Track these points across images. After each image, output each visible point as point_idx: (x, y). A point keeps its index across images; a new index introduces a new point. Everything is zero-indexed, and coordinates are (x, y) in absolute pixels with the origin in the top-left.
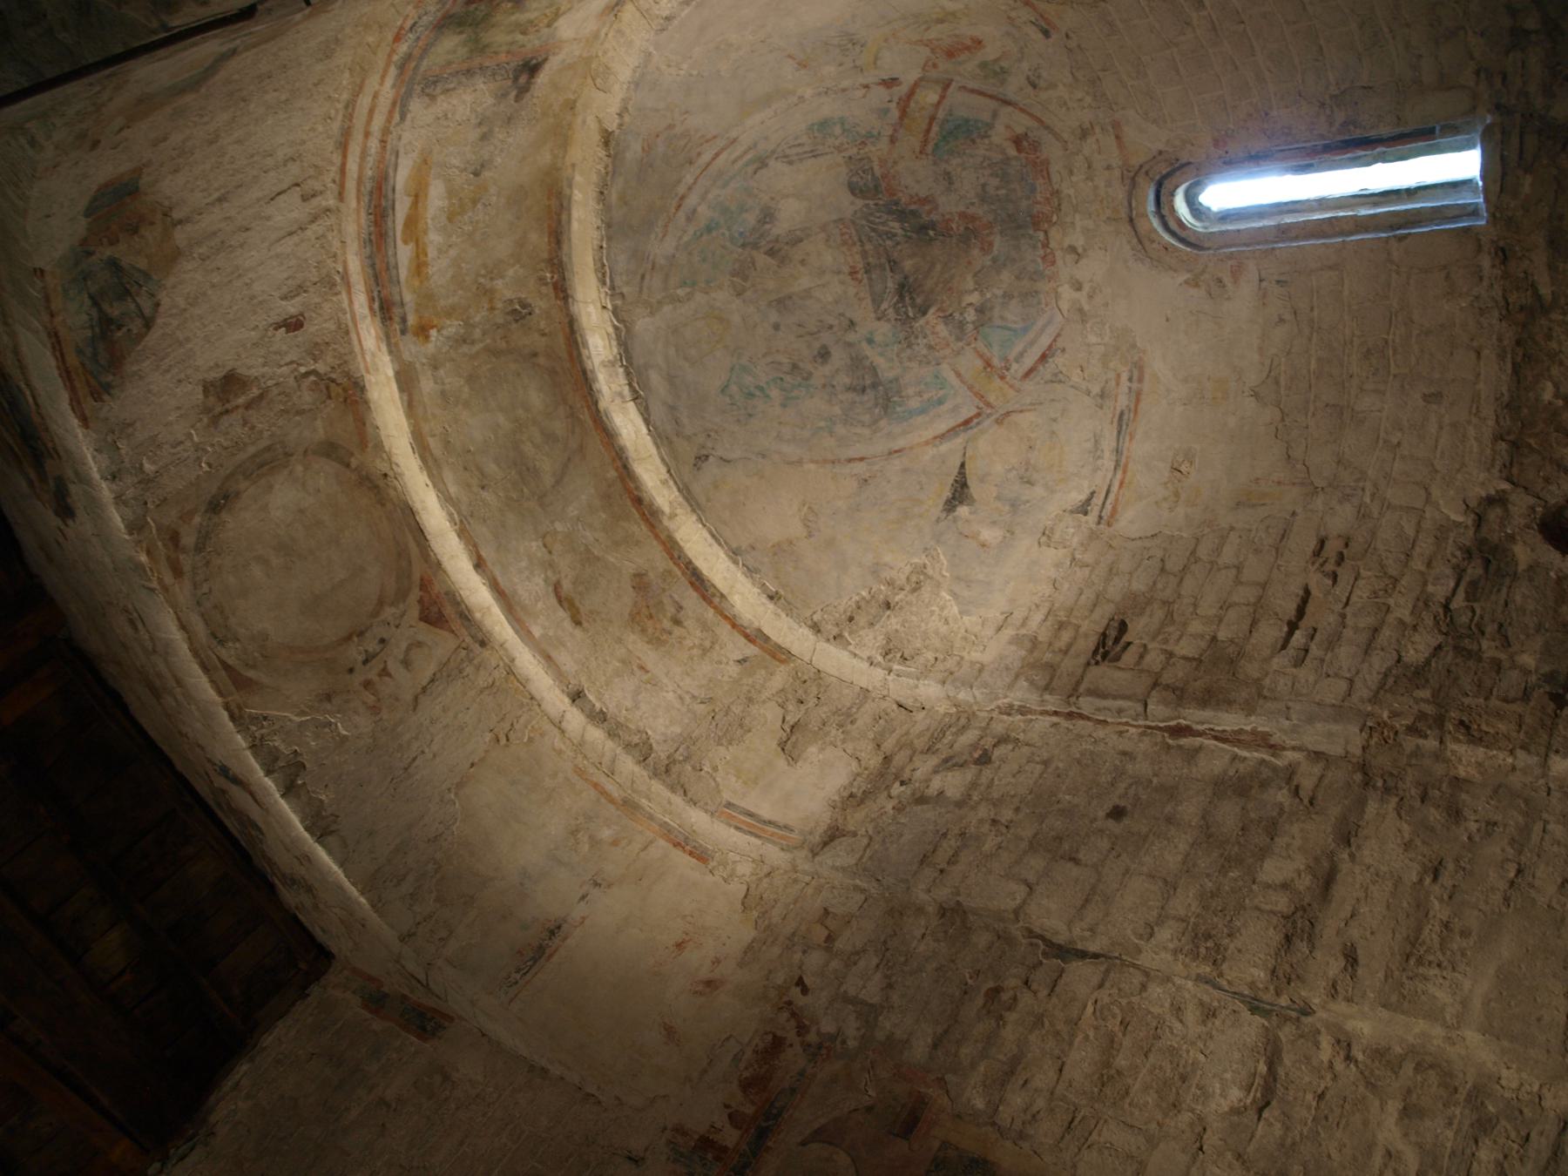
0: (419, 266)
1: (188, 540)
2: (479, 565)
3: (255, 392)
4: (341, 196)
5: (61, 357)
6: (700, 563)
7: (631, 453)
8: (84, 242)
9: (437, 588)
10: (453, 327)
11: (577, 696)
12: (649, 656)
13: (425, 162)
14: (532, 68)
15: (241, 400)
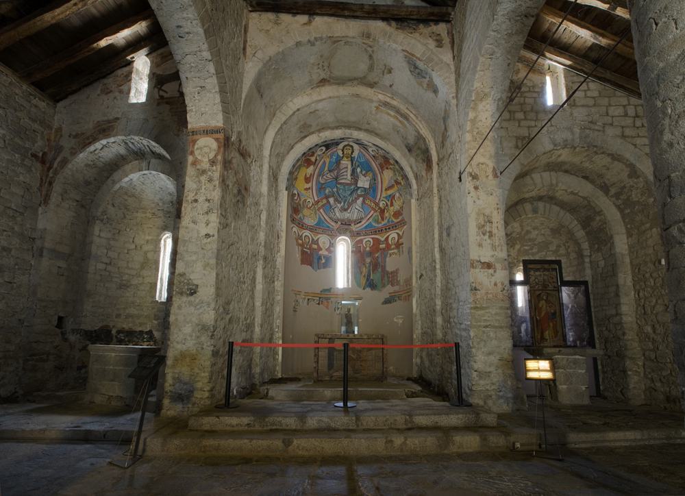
0: (389, 114)
1: (369, 49)
2: (330, 98)
3: (385, 74)
4: (407, 108)
5: (417, 58)
6: (307, 139)
7: (333, 131)
8: (432, 79)
9: (327, 83)
10: (374, 112)
11: (298, 110)
12: (298, 126)
13: (405, 126)
14: (410, 151)
15: (386, 71)
